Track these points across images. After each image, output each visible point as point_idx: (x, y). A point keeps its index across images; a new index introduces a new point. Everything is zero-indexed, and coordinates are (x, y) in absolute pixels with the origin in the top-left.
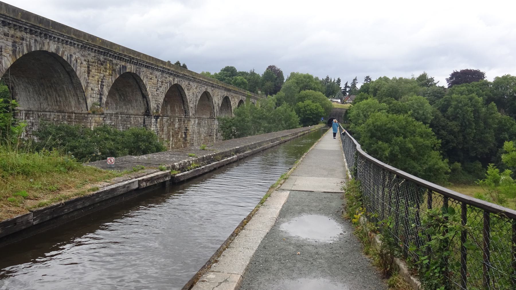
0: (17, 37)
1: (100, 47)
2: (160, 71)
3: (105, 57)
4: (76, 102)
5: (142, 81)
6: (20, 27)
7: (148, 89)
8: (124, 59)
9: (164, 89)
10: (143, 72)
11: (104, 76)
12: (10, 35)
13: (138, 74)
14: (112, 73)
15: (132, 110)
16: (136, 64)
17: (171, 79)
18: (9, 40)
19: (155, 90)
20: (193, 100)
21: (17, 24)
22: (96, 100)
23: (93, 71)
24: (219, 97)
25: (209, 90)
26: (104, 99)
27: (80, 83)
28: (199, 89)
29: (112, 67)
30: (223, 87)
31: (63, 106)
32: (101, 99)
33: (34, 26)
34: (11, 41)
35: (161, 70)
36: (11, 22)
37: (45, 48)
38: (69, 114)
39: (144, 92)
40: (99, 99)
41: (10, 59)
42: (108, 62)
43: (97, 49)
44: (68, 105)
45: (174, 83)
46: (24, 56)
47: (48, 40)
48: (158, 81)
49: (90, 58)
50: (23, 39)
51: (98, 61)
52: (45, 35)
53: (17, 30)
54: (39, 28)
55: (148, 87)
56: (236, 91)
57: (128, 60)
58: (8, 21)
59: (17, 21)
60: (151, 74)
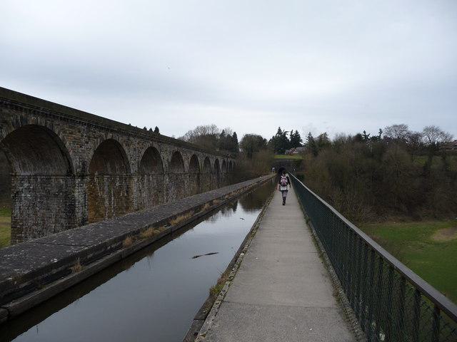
8: (21, 108)
25: (155, 145)
48: (82, 136)
60: (71, 127)
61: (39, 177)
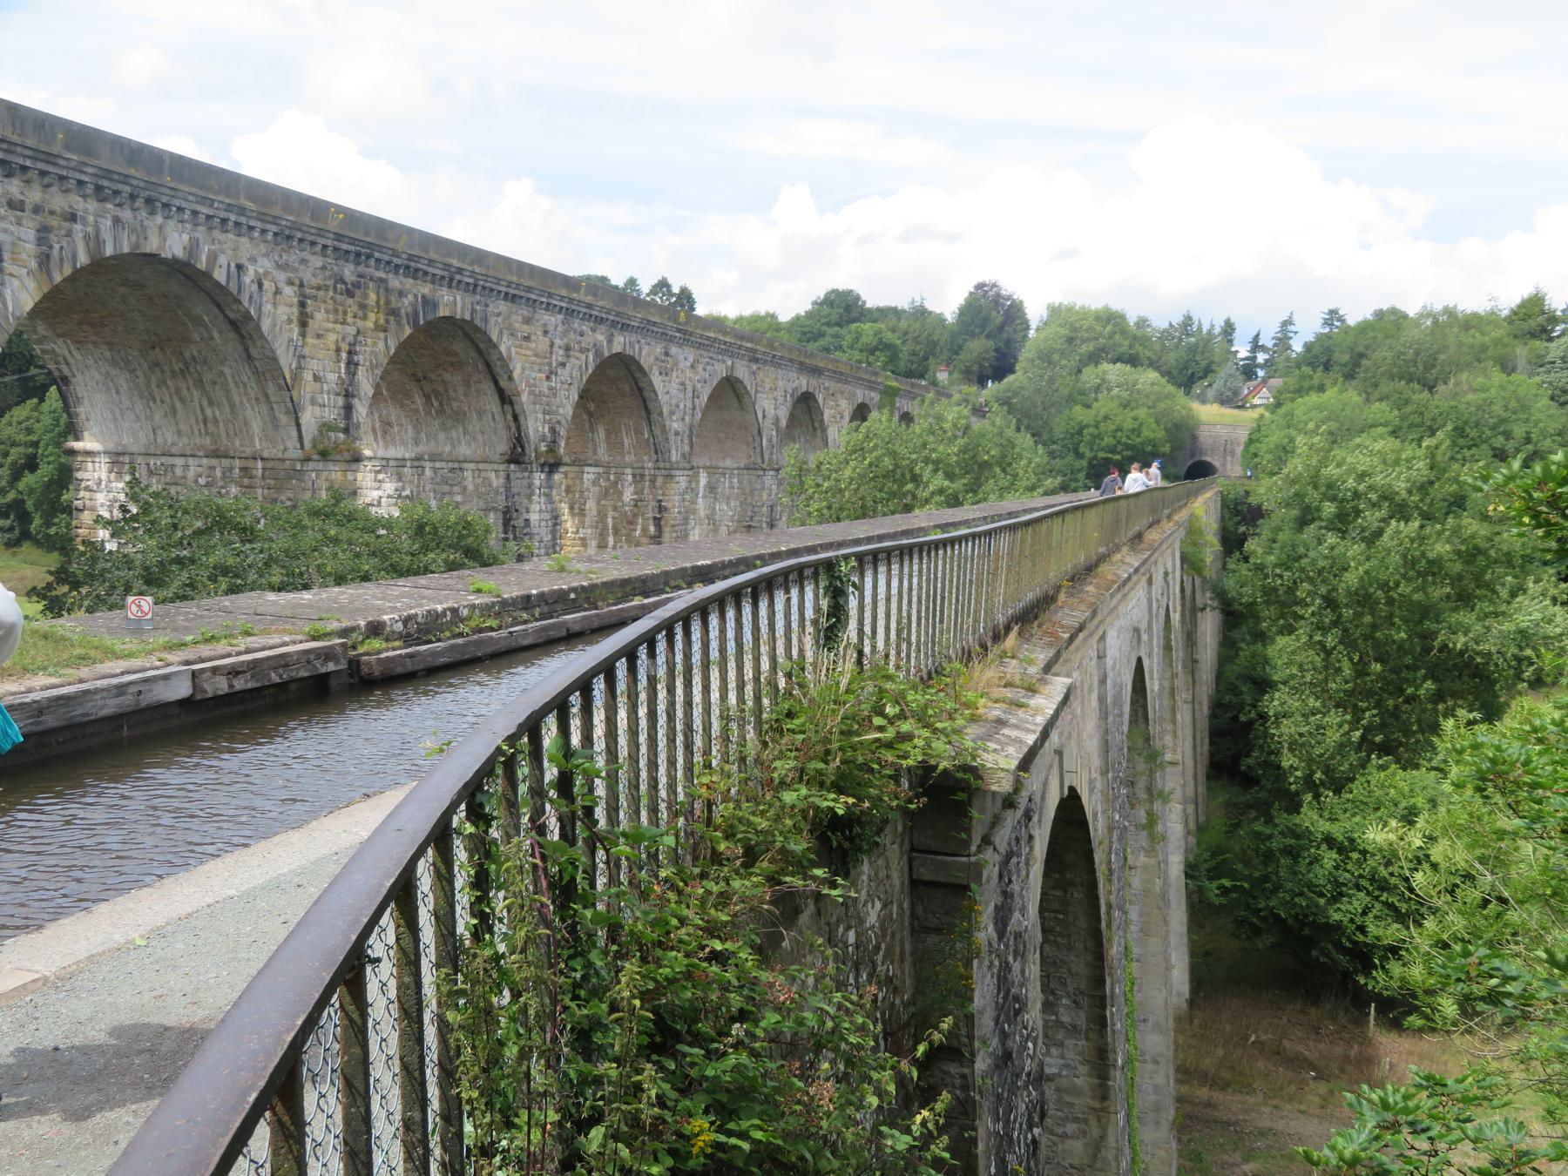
0: (52, 213)
1: (339, 237)
2: (560, 312)
3: (361, 269)
4: (265, 422)
5: (495, 346)
6: (62, 178)
7: (516, 374)
8: (426, 273)
9: (578, 370)
10: (498, 315)
11: (358, 332)
12: (28, 207)
13: (478, 322)
14: (387, 321)
15: (468, 444)
16: (471, 289)
17: (601, 337)
18: (24, 222)
19: (544, 376)
20: (682, 406)
21: (51, 169)
22: (332, 415)
23: (320, 318)
24: (779, 393)
25: (742, 372)
26: (361, 410)
27: (275, 360)
28: (705, 370)
29: (388, 302)
30: (791, 360)
31: (223, 434)
32: (348, 409)
33: (107, 174)
34: (31, 224)
35: (561, 308)
36: (28, 163)
37: (152, 246)
38: (245, 463)
39: (503, 384)
40: (342, 412)
41: (31, 284)
42: (371, 285)
43: (329, 243)
44: (241, 431)
45: (610, 349)
46: (77, 275)
47: (159, 219)
48: (552, 345)
49: (307, 275)
50: (73, 218)
51: (336, 282)
52: (149, 201)
53: (54, 189)
54: (125, 179)
55: (518, 366)
56: (842, 374)
57: (443, 277)
58: (20, 161)
59: (50, 158)
60: (527, 321)
61: (428, 464)
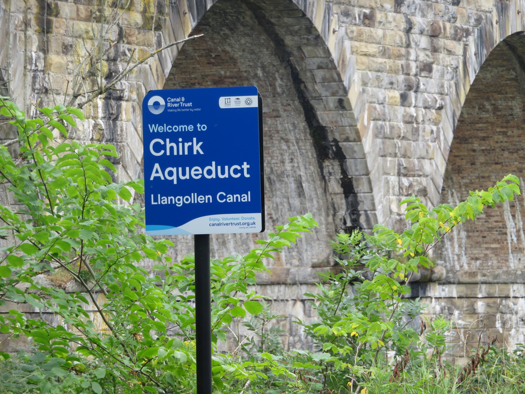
7: (353, 96)
11: (121, 35)
45: (503, 28)
48: (408, 31)
55: (357, 77)
